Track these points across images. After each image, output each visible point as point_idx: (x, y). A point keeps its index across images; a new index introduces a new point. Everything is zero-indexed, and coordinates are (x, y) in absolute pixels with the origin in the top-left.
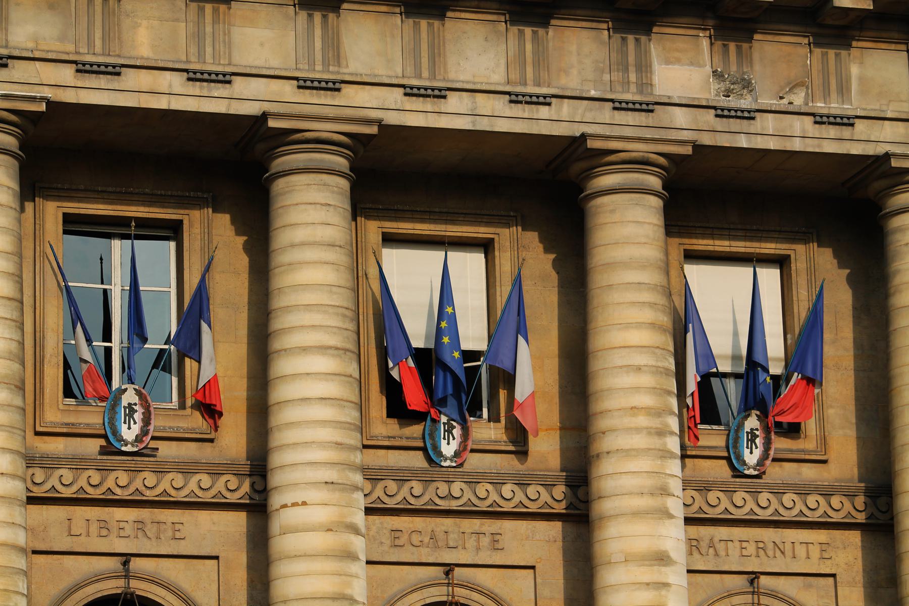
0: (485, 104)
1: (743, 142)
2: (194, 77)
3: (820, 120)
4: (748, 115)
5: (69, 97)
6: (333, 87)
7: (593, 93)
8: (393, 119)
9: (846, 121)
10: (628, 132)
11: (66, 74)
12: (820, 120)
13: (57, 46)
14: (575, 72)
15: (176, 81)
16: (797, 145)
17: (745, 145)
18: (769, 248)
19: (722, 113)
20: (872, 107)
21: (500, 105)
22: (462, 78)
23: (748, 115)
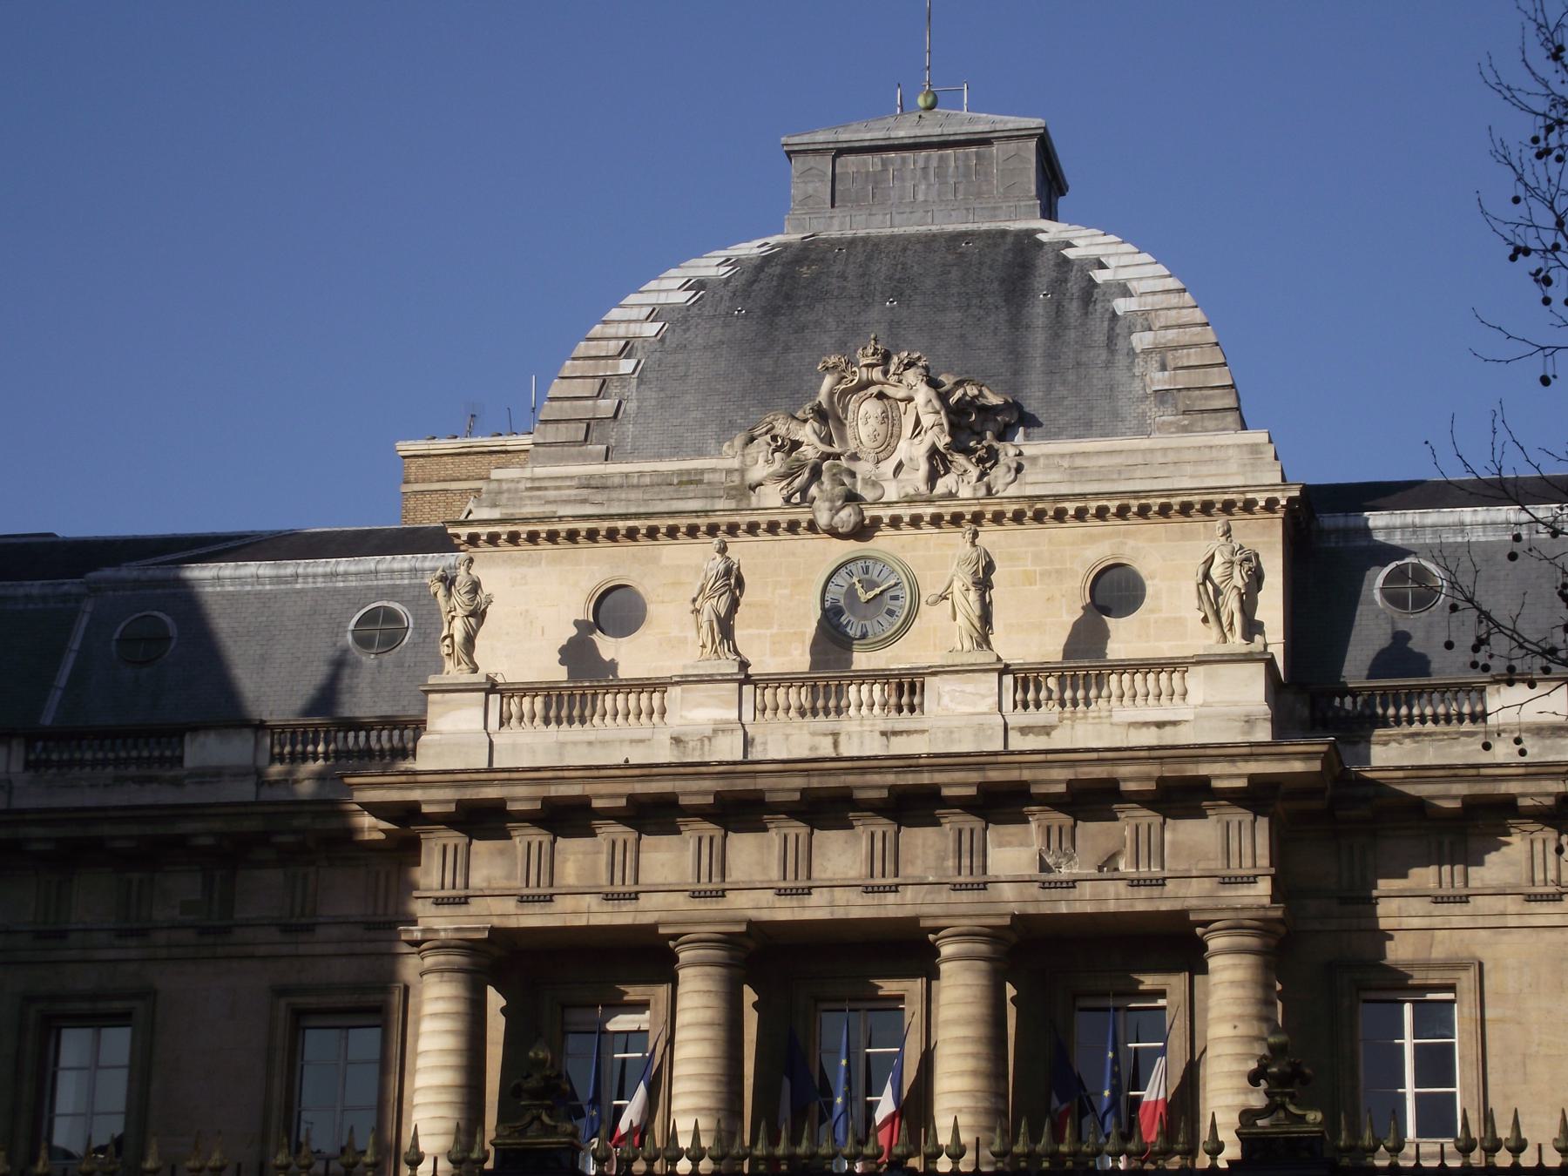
0: (841, 896)
1: (1063, 908)
5: (513, 923)
7: (931, 879)
8: (766, 915)
10: (963, 909)
11: (510, 905)
12: (1135, 883)
13: (504, 883)
14: (919, 862)
15: (591, 901)
16: (1112, 907)
17: (1064, 911)
21: (854, 896)
22: (824, 876)
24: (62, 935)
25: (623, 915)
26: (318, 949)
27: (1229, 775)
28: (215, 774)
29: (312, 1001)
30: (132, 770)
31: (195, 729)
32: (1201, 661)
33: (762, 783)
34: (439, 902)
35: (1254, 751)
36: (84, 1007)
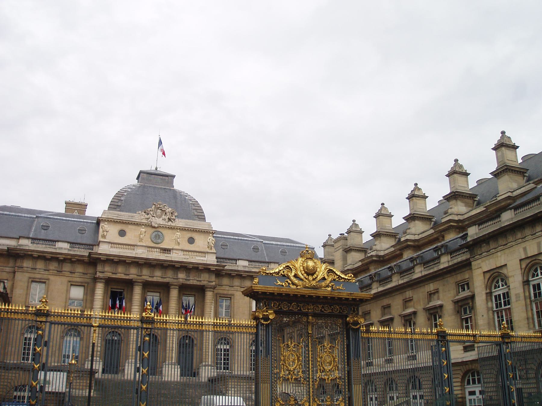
2: (125, 274)
3: (197, 281)
4: (189, 280)
6: (141, 276)
9: (201, 281)
11: (111, 274)
12: (197, 281)
15: (123, 275)
18: (193, 293)
19: (186, 280)
20: (204, 279)
23: (189, 280)
24: (36, 269)
25: (127, 277)
27: (213, 268)
28: (62, 248)
29: (74, 284)
30: (48, 246)
31: (58, 241)
32: (208, 253)
33: (151, 261)
34: (100, 272)
35: (217, 265)
36: (39, 280)
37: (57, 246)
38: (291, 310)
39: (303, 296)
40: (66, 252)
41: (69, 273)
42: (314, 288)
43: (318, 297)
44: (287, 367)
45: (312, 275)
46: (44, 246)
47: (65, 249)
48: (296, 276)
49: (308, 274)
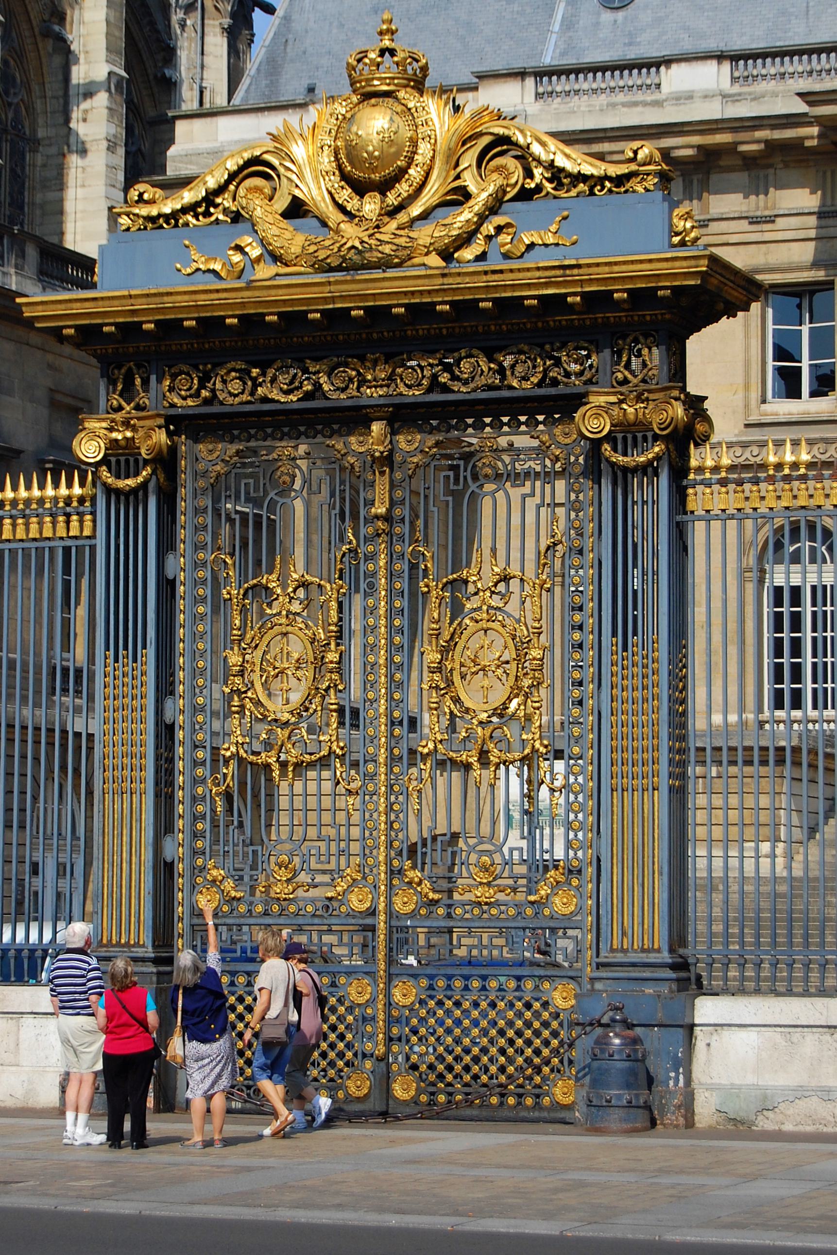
26: (779, 236)
28: (689, 97)
30: (620, 97)
31: (668, 62)
37: (664, 88)
38: (265, 400)
39: (293, 319)
40: (713, 111)
41: (744, 225)
42: (351, 264)
43: (378, 314)
44: (258, 703)
45: (384, 187)
46: (603, 99)
47: (707, 96)
48: (296, 210)
49: (360, 189)
